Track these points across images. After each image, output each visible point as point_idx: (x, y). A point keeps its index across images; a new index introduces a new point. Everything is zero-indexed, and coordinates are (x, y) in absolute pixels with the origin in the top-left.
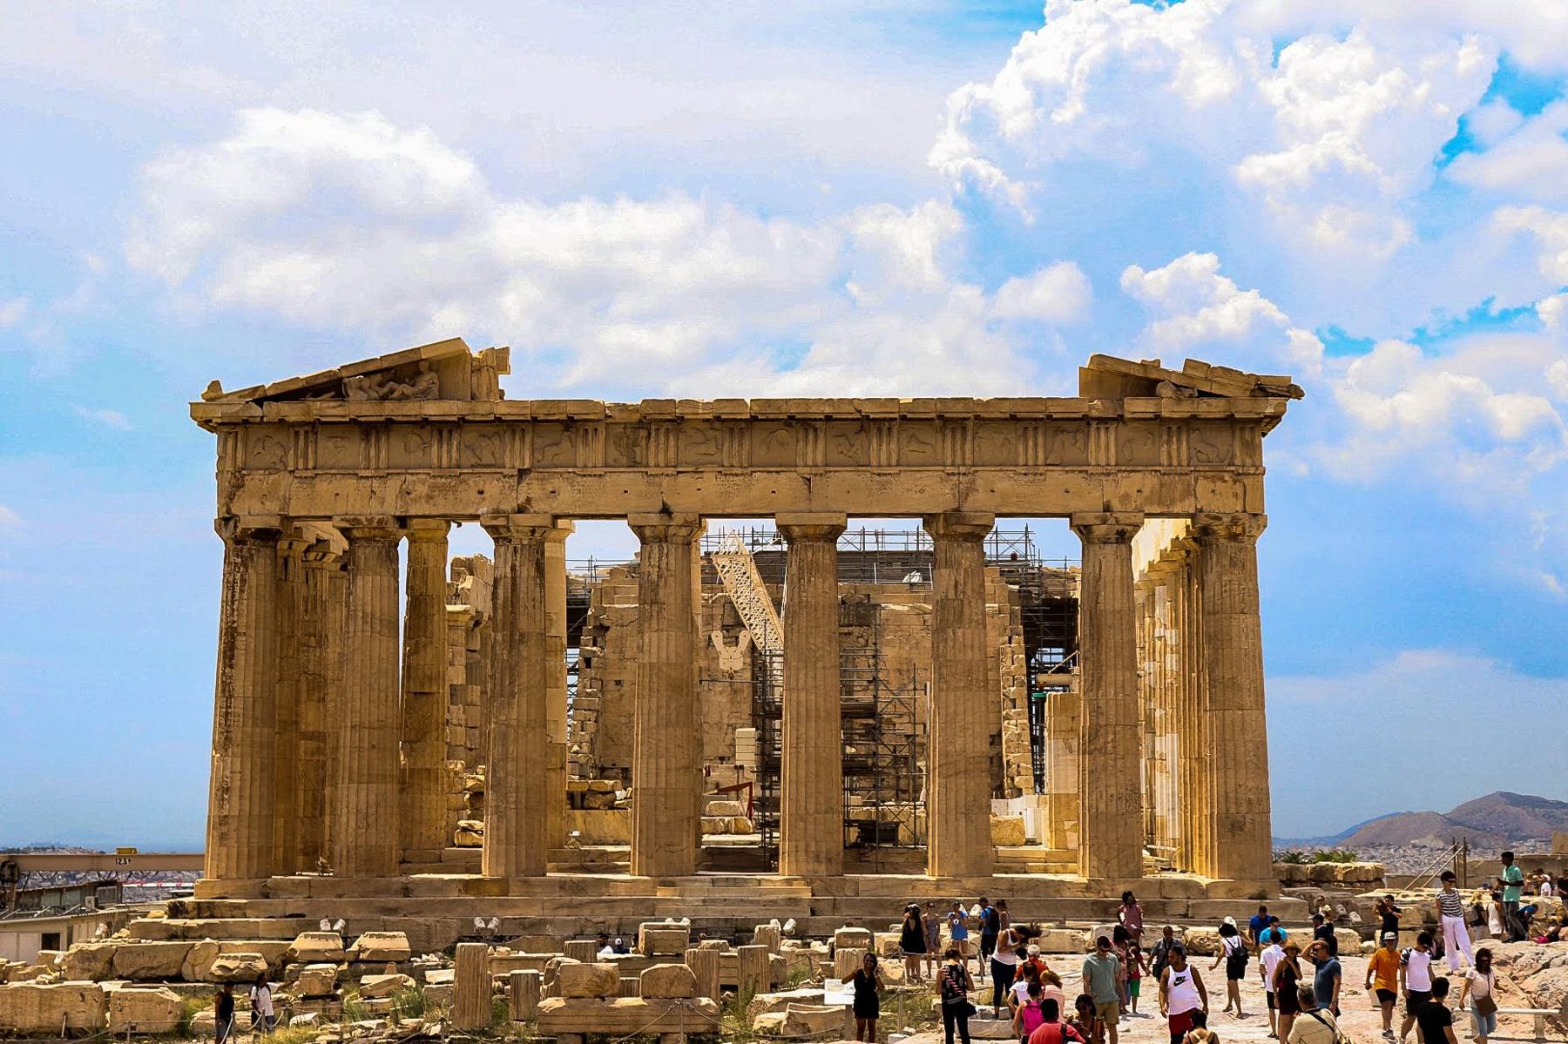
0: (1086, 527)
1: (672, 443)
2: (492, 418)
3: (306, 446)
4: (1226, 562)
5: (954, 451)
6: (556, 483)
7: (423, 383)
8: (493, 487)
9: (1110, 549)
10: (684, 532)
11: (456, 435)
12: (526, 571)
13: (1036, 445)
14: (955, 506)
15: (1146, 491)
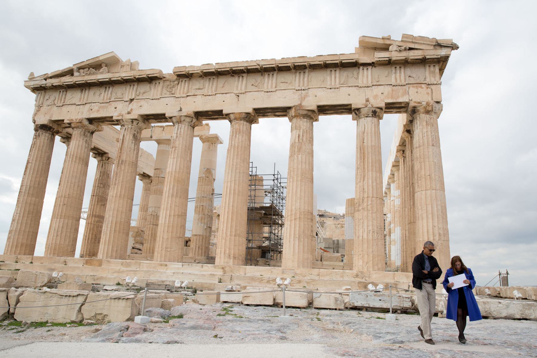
0: (358, 109)
1: (186, 85)
2: (119, 79)
3: (62, 96)
4: (425, 123)
5: (299, 82)
6: (142, 103)
7: (101, 70)
9: (369, 119)
10: (188, 120)
11: (111, 89)
12: (129, 137)
13: (335, 77)
14: (300, 103)
15: (386, 93)
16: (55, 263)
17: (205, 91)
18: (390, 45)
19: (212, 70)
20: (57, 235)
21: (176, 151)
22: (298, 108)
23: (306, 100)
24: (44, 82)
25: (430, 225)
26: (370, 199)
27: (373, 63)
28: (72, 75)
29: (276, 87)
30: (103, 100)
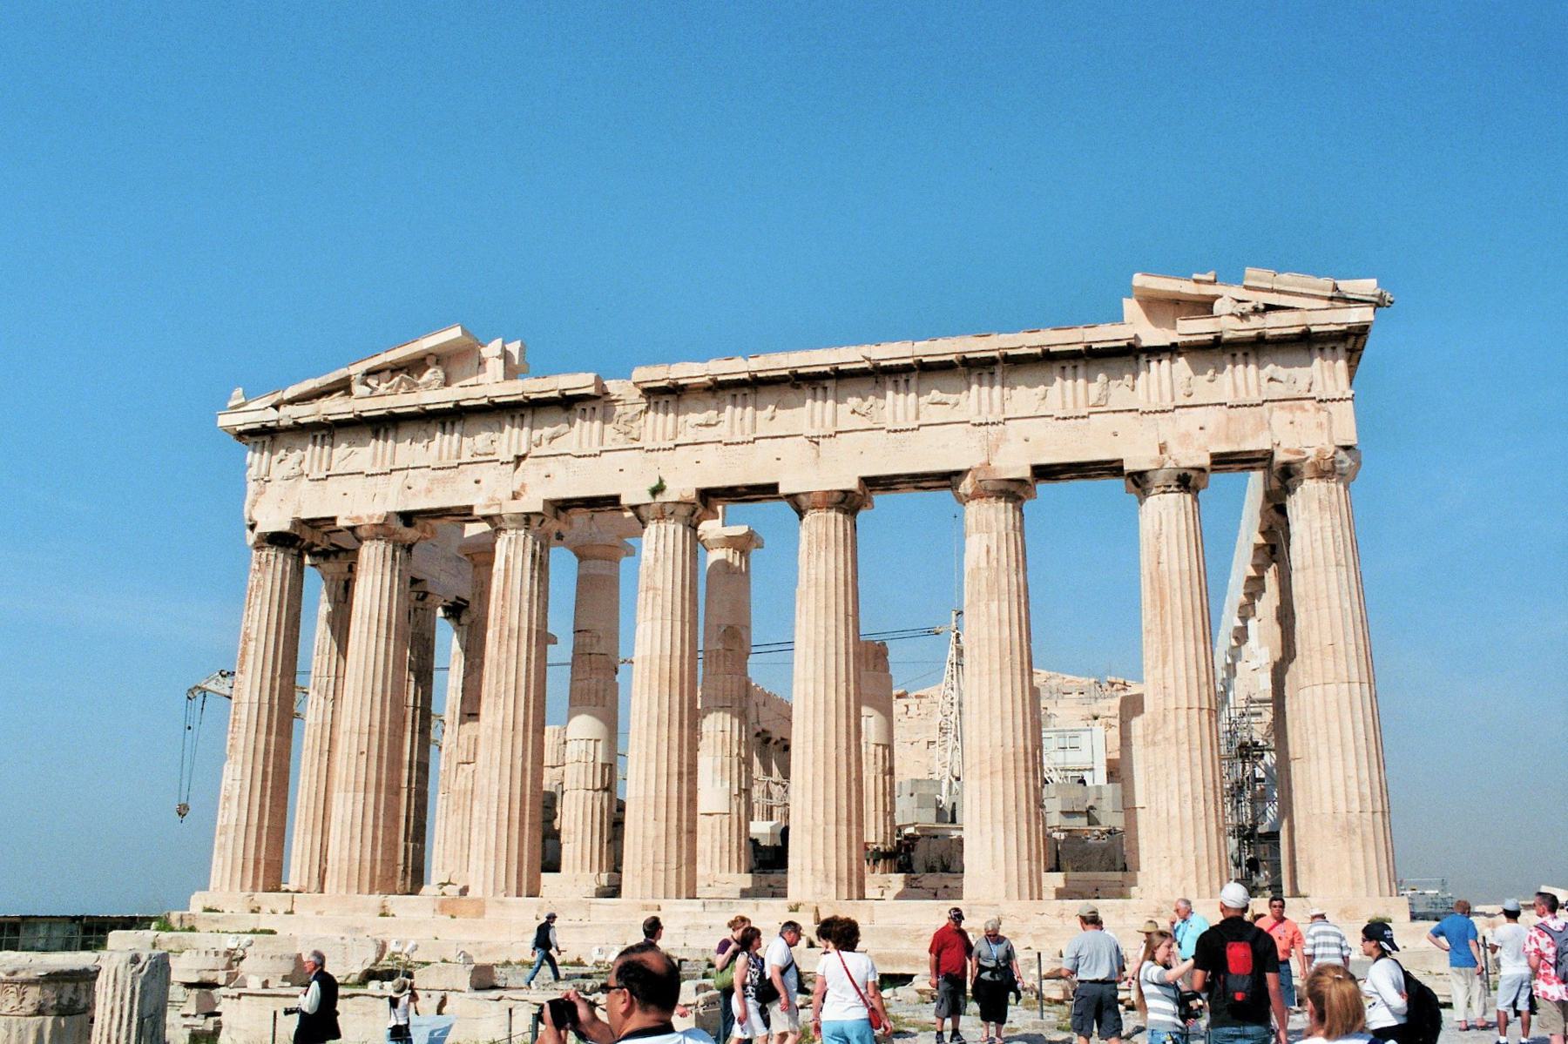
2: (485, 401)
4: (1315, 506)
6: (551, 465)
7: (427, 376)
8: (487, 473)
14: (984, 459)
16: (355, 910)
17: (721, 432)
18: (1217, 297)
19: (741, 376)
20: (352, 838)
21: (659, 600)
22: (981, 476)
23: (1001, 451)
24: (272, 415)
25: (1339, 773)
26: (1183, 713)
27: (1174, 345)
28: (349, 393)
29: (917, 418)
30: (440, 458)
